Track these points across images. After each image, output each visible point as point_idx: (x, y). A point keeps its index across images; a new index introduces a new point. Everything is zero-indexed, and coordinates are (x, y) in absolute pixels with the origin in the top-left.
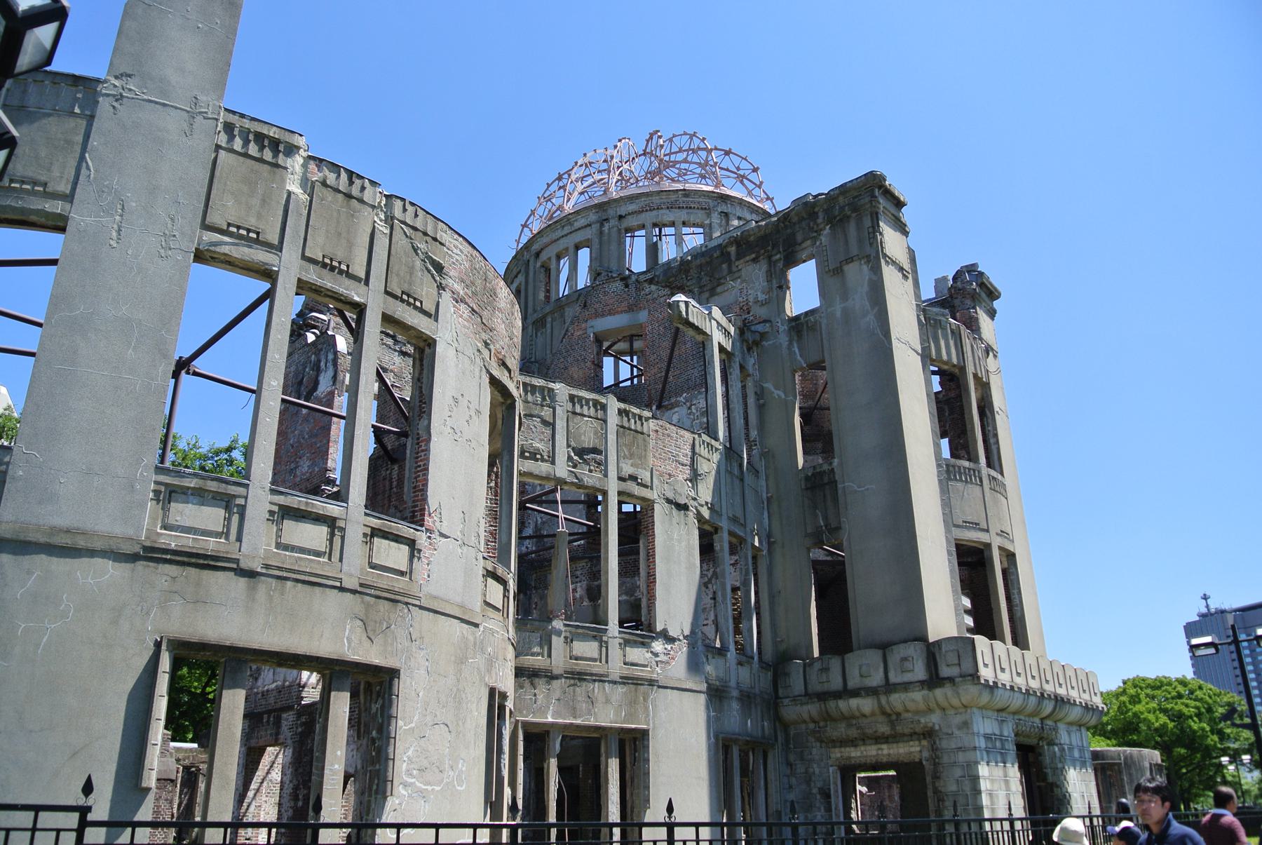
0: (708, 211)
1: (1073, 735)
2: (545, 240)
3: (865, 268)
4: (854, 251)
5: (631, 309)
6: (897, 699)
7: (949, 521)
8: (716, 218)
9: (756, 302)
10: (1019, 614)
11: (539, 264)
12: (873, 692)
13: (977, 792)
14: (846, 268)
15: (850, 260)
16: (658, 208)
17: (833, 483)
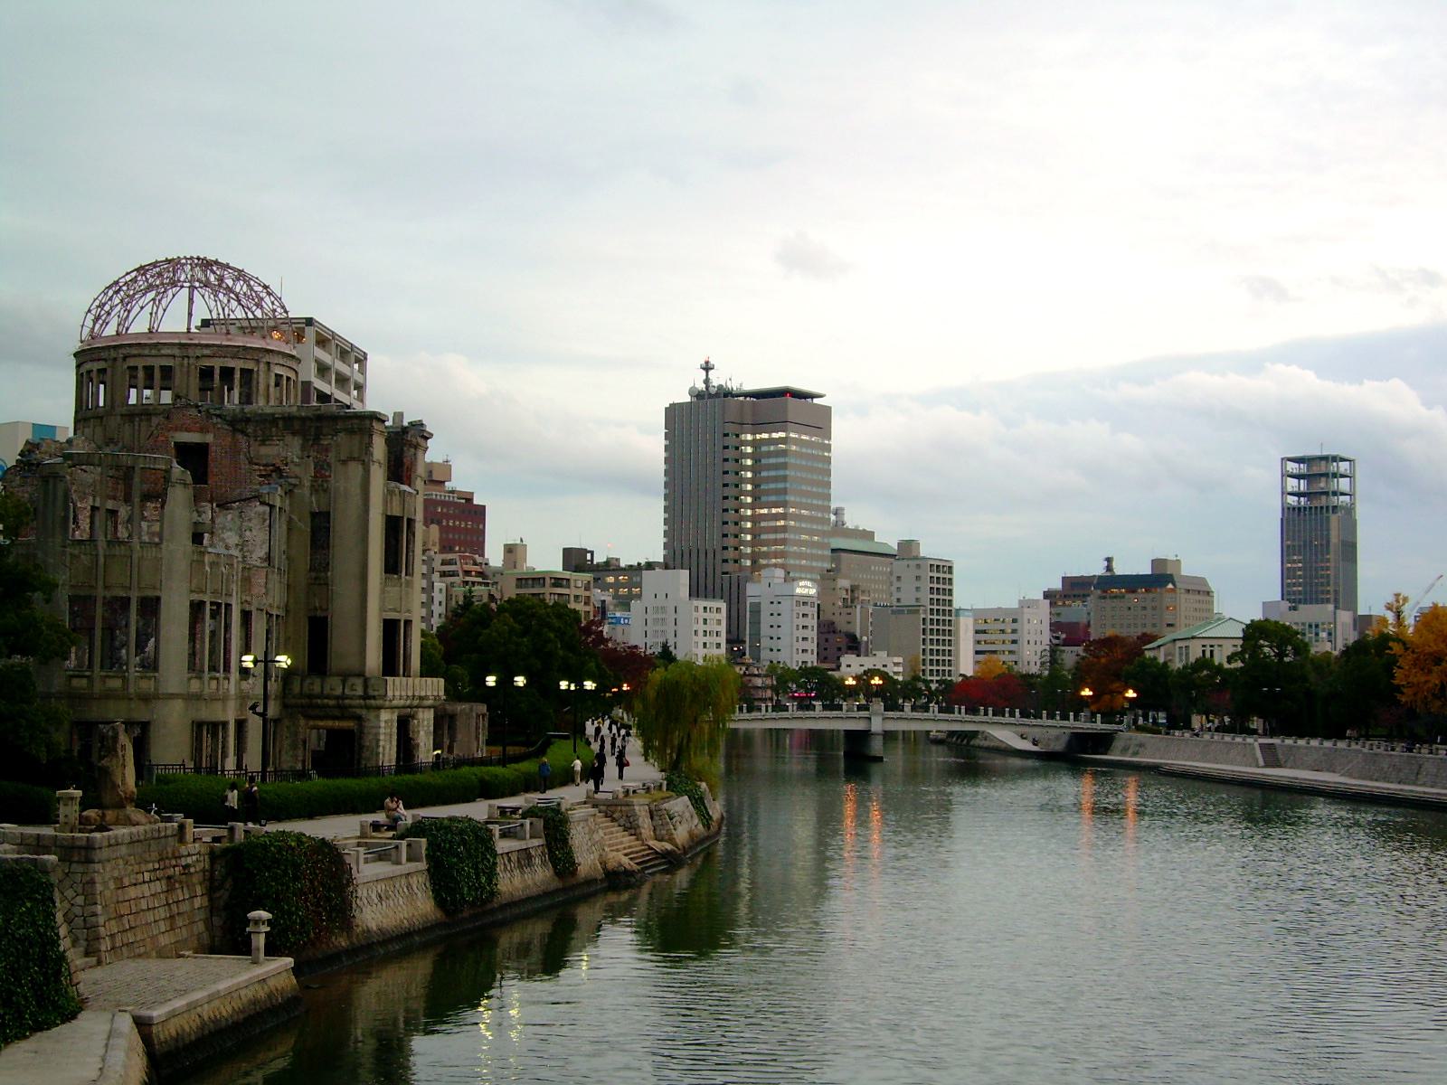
0: (258, 361)
1: (425, 713)
2: (134, 351)
3: (360, 466)
4: (356, 456)
5: (203, 430)
6: (347, 701)
7: (382, 609)
8: (262, 366)
9: (293, 462)
10: (409, 653)
11: (126, 367)
12: (337, 698)
13: (378, 746)
14: (349, 462)
15: (353, 459)
16: (225, 357)
17: (327, 584)
